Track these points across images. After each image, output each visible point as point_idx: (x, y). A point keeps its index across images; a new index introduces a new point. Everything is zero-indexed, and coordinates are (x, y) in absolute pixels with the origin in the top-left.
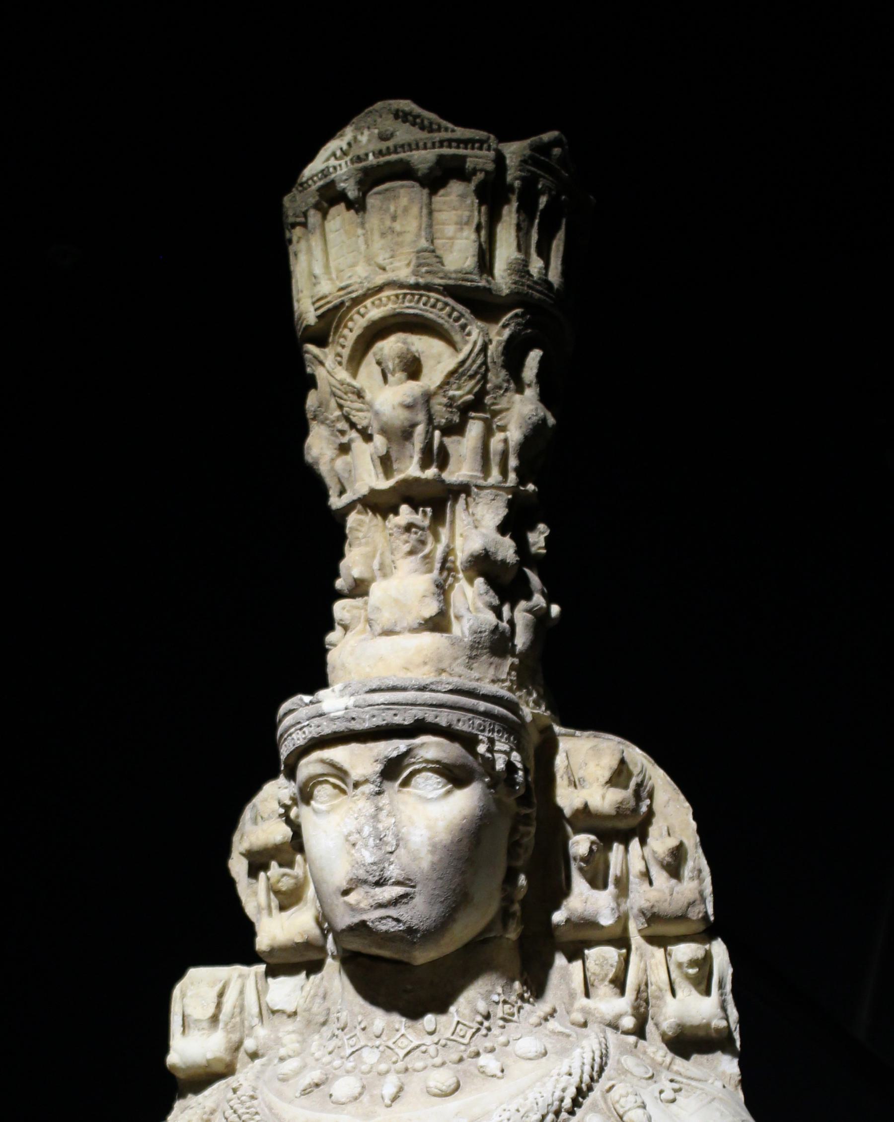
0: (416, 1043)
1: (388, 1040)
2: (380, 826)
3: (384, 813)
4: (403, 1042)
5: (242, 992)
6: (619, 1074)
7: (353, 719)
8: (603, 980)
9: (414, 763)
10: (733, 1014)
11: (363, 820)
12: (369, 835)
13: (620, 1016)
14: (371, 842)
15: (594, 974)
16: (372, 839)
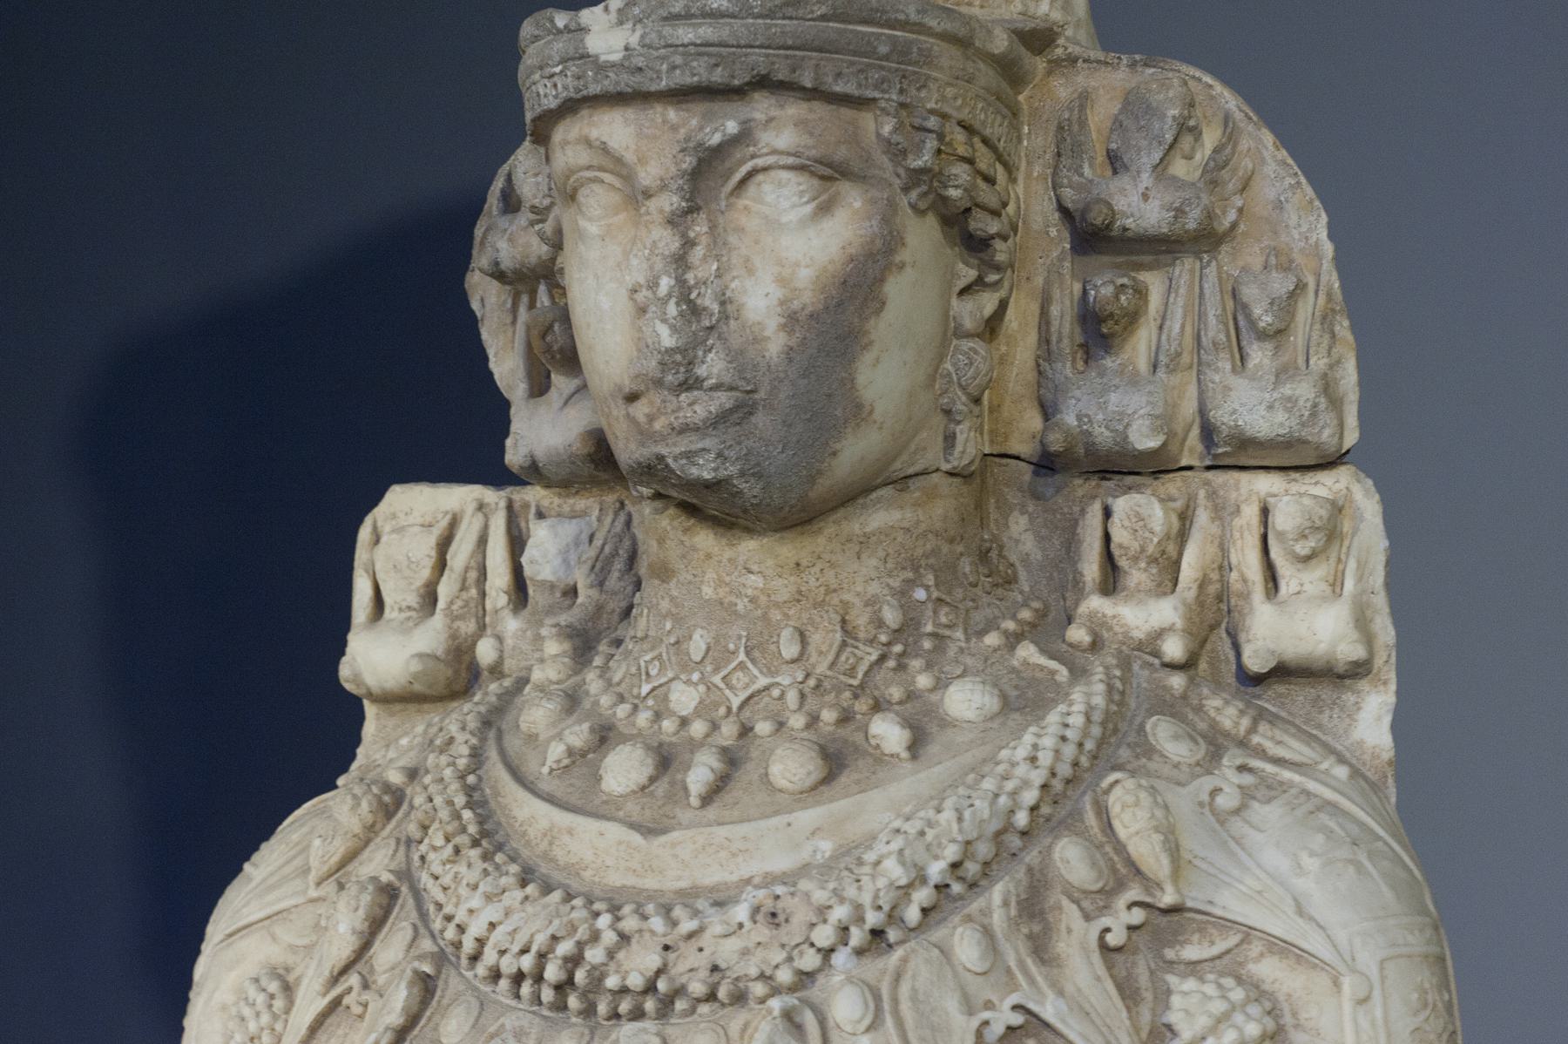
0: (763, 681)
1: (717, 670)
2: (690, 277)
3: (698, 253)
4: (739, 679)
5: (483, 541)
6: (1137, 757)
7: (640, 69)
8: (1136, 559)
9: (753, 157)
10: (1385, 631)
11: (659, 265)
12: (669, 296)
13: (1160, 634)
14: (672, 310)
15: (1120, 546)
16: (673, 300)
